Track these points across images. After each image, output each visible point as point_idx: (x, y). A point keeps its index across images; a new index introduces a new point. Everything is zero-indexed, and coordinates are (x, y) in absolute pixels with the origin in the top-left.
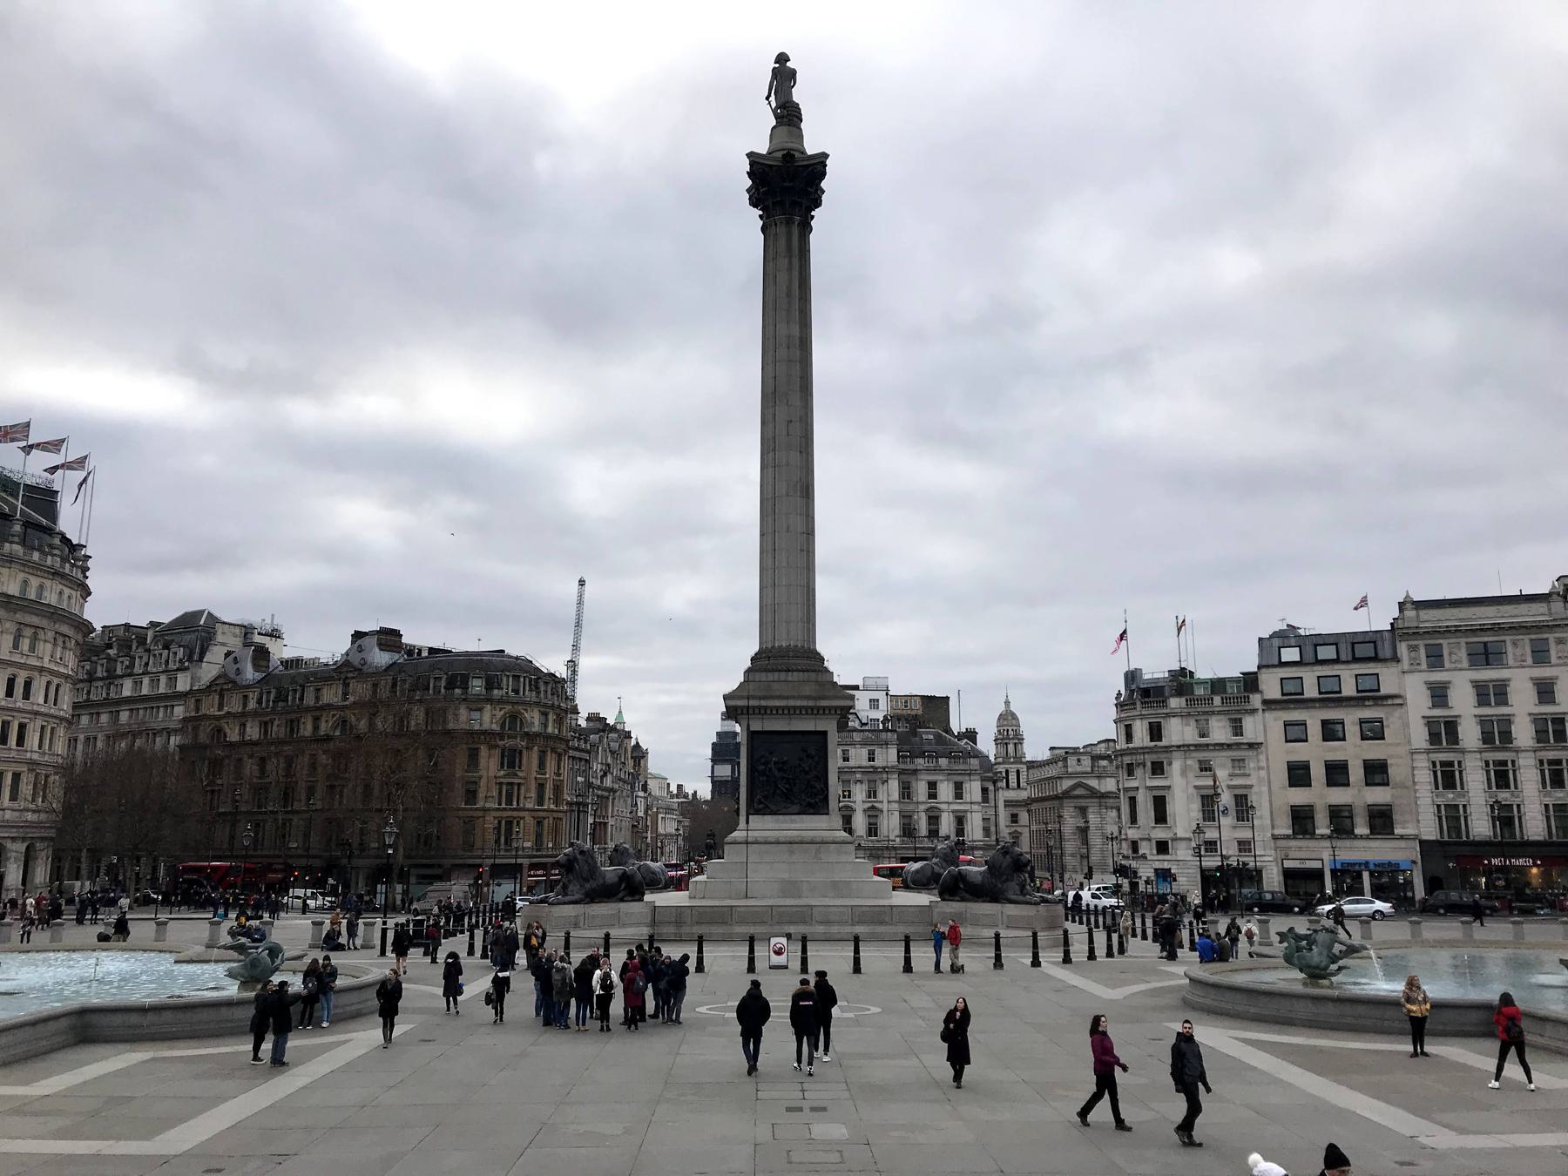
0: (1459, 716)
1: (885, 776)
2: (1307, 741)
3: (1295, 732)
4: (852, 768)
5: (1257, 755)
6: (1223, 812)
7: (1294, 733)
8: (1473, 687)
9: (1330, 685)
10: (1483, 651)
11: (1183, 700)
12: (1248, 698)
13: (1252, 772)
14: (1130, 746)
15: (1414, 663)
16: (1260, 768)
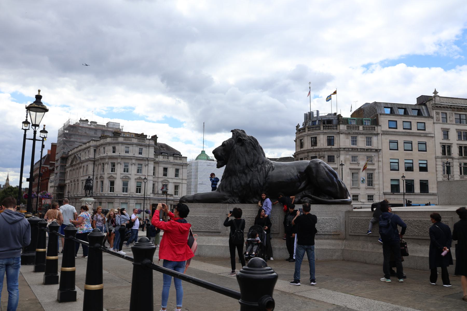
0: (452, 144)
1: (147, 162)
2: (397, 150)
3: (394, 145)
4: (131, 157)
5: (378, 155)
6: (362, 181)
7: (394, 145)
8: (457, 132)
9: (407, 125)
10: (459, 118)
11: (346, 126)
12: (374, 128)
13: (376, 164)
14: (315, 147)
15: (438, 120)
16: (379, 161)
